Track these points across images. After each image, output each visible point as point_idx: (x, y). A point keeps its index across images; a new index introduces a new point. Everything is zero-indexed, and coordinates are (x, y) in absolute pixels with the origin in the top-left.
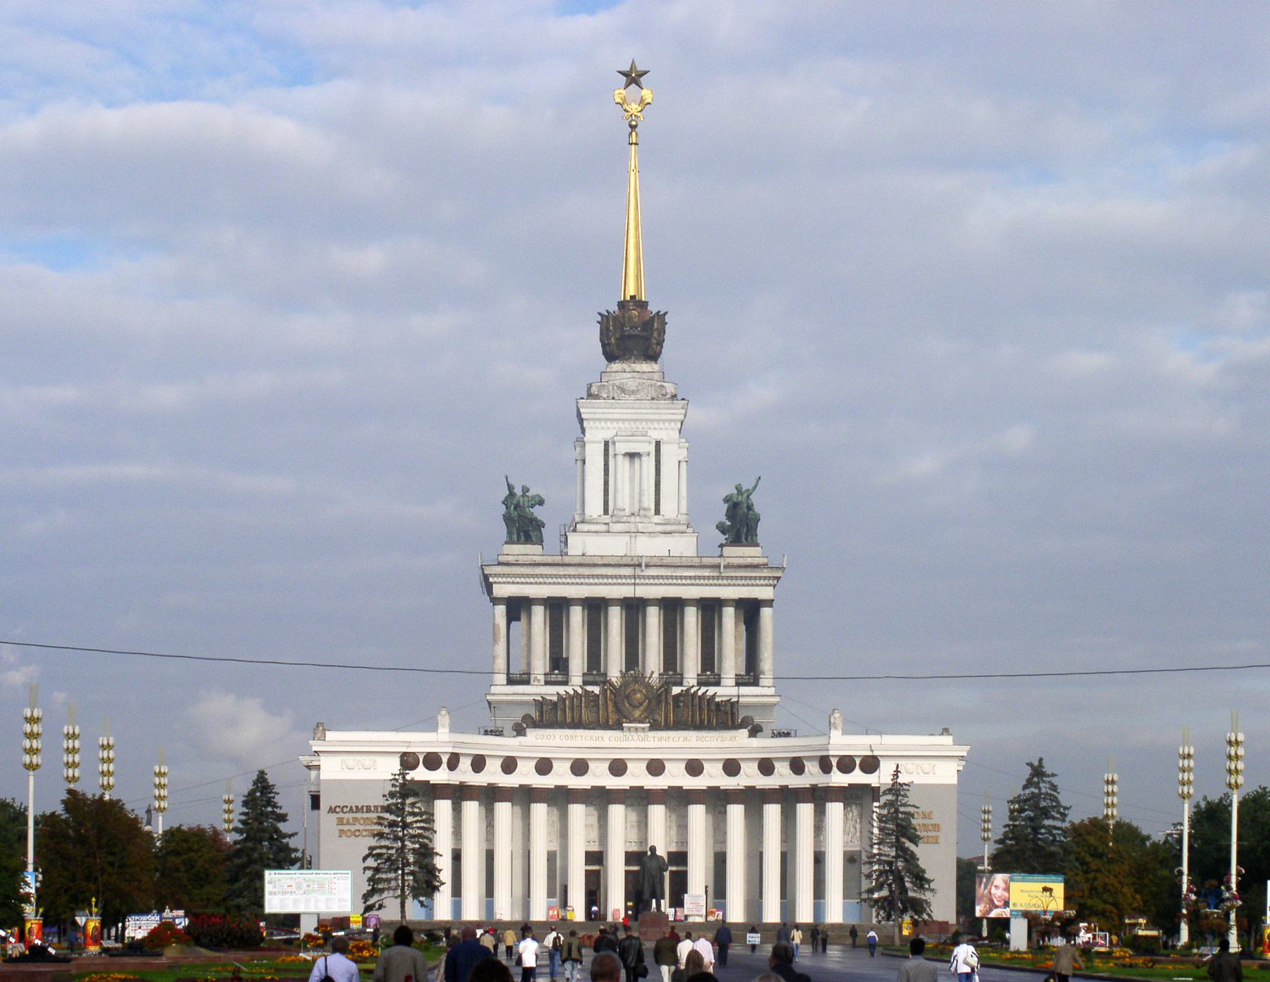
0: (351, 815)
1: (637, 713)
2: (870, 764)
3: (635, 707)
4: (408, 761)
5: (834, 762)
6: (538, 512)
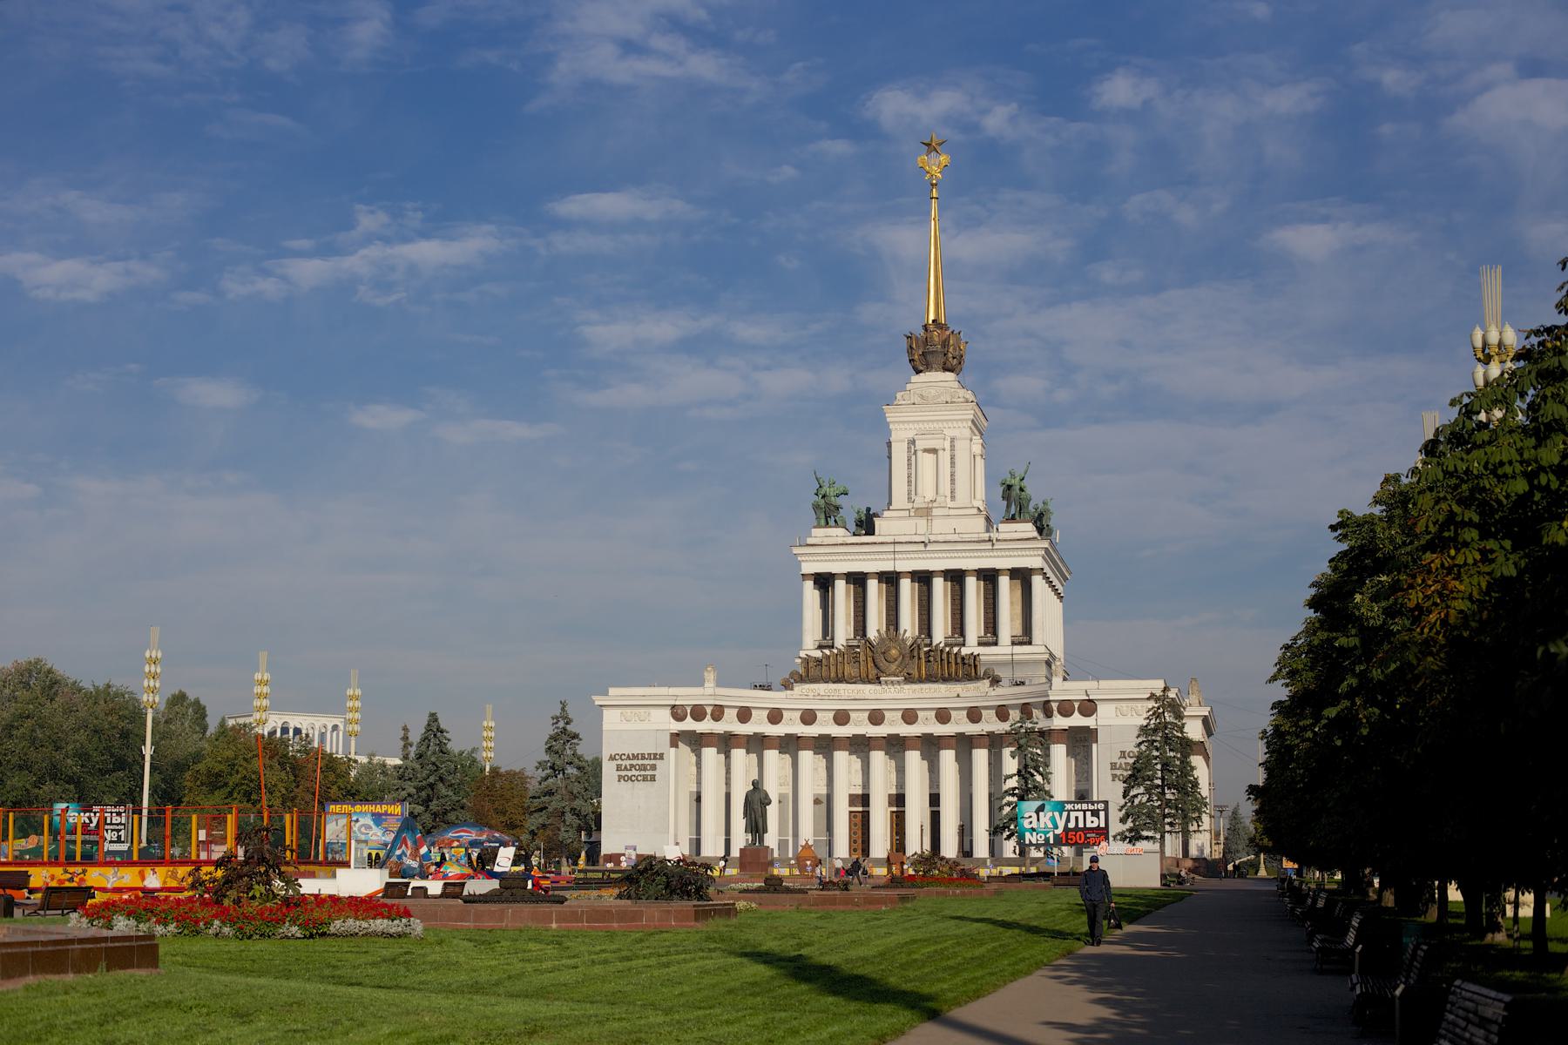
0: (628, 763)
1: (893, 667)
2: (1088, 707)
5: (1055, 706)
6: (840, 501)
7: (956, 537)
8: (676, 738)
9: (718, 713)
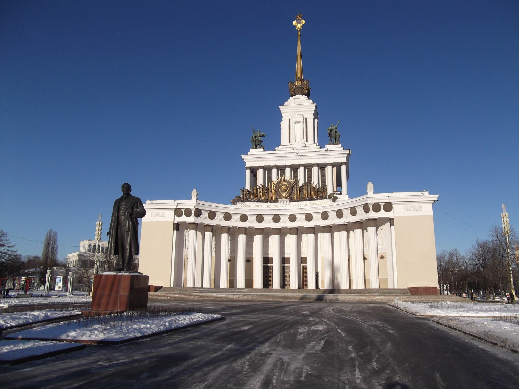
2: (388, 207)
3: (284, 192)
7: (310, 150)
8: (177, 227)
9: (198, 213)
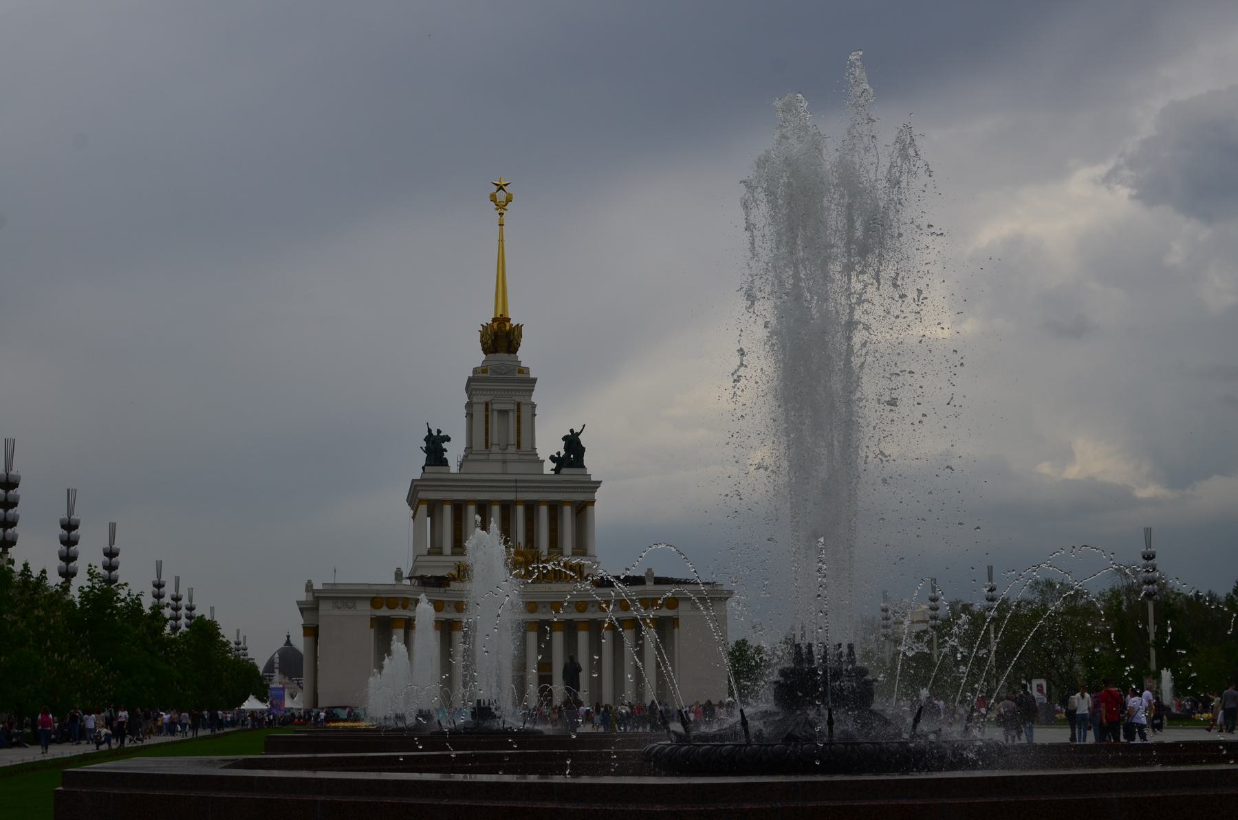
4: (376, 602)
6: (445, 445)
